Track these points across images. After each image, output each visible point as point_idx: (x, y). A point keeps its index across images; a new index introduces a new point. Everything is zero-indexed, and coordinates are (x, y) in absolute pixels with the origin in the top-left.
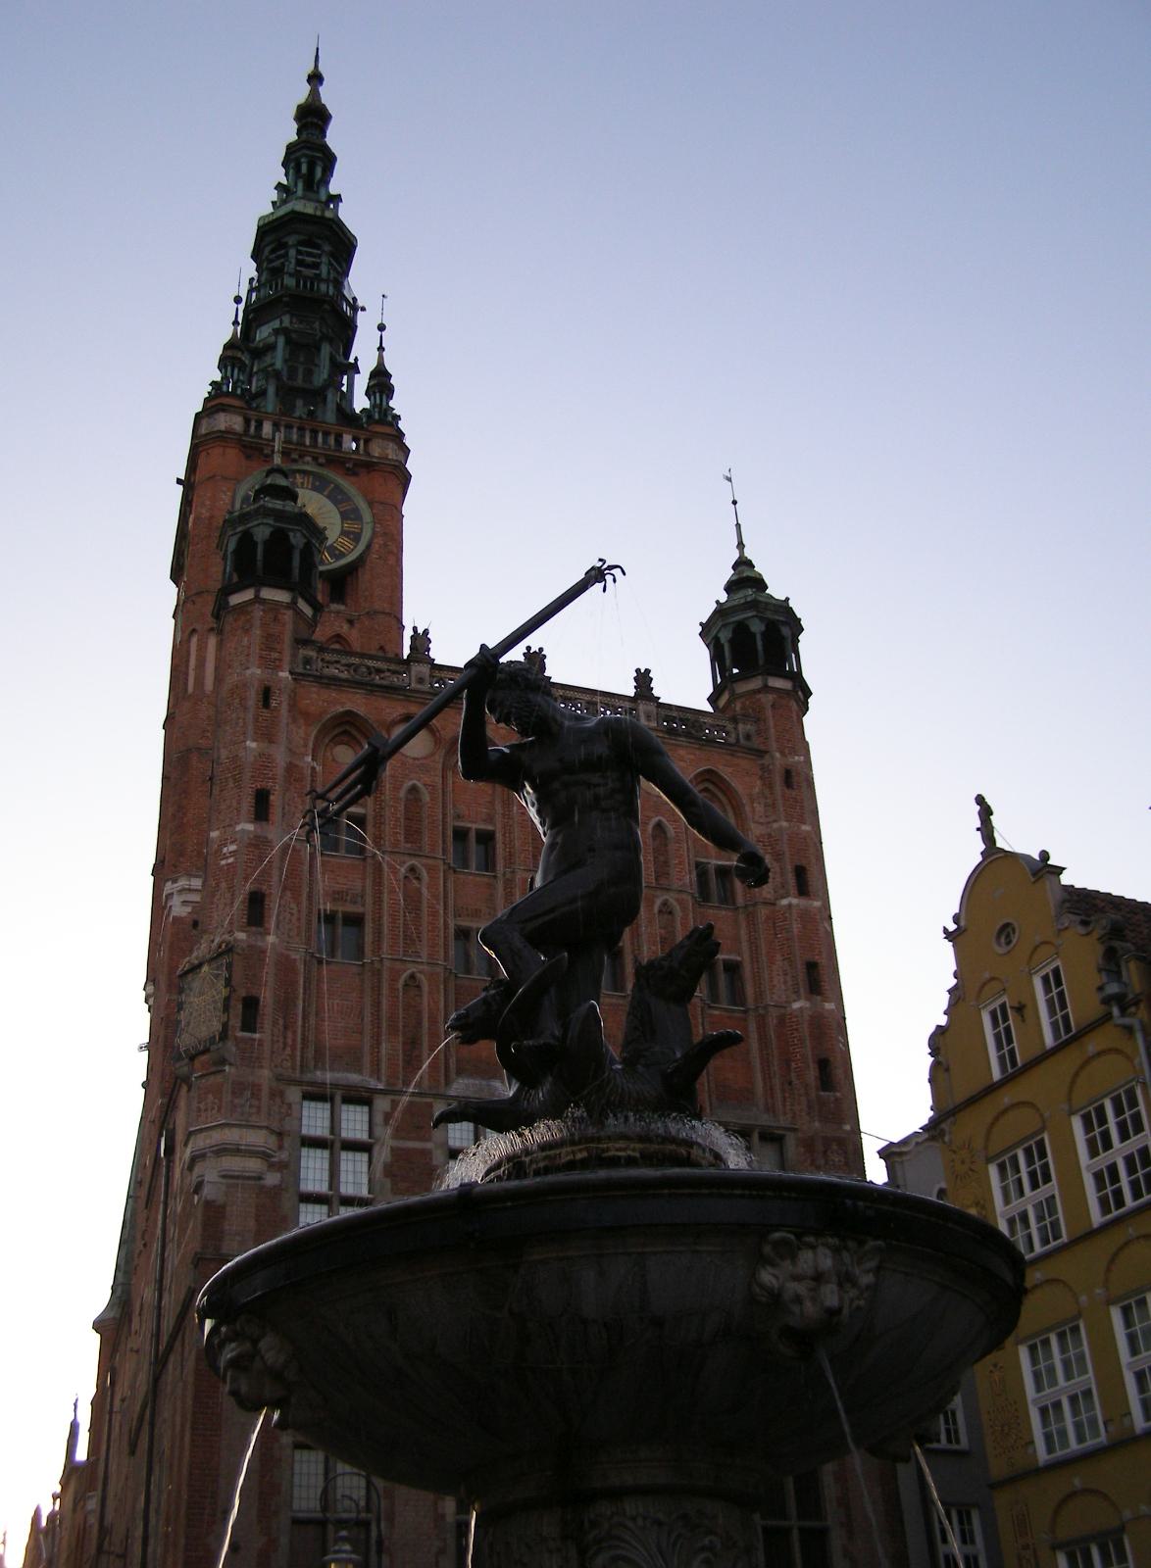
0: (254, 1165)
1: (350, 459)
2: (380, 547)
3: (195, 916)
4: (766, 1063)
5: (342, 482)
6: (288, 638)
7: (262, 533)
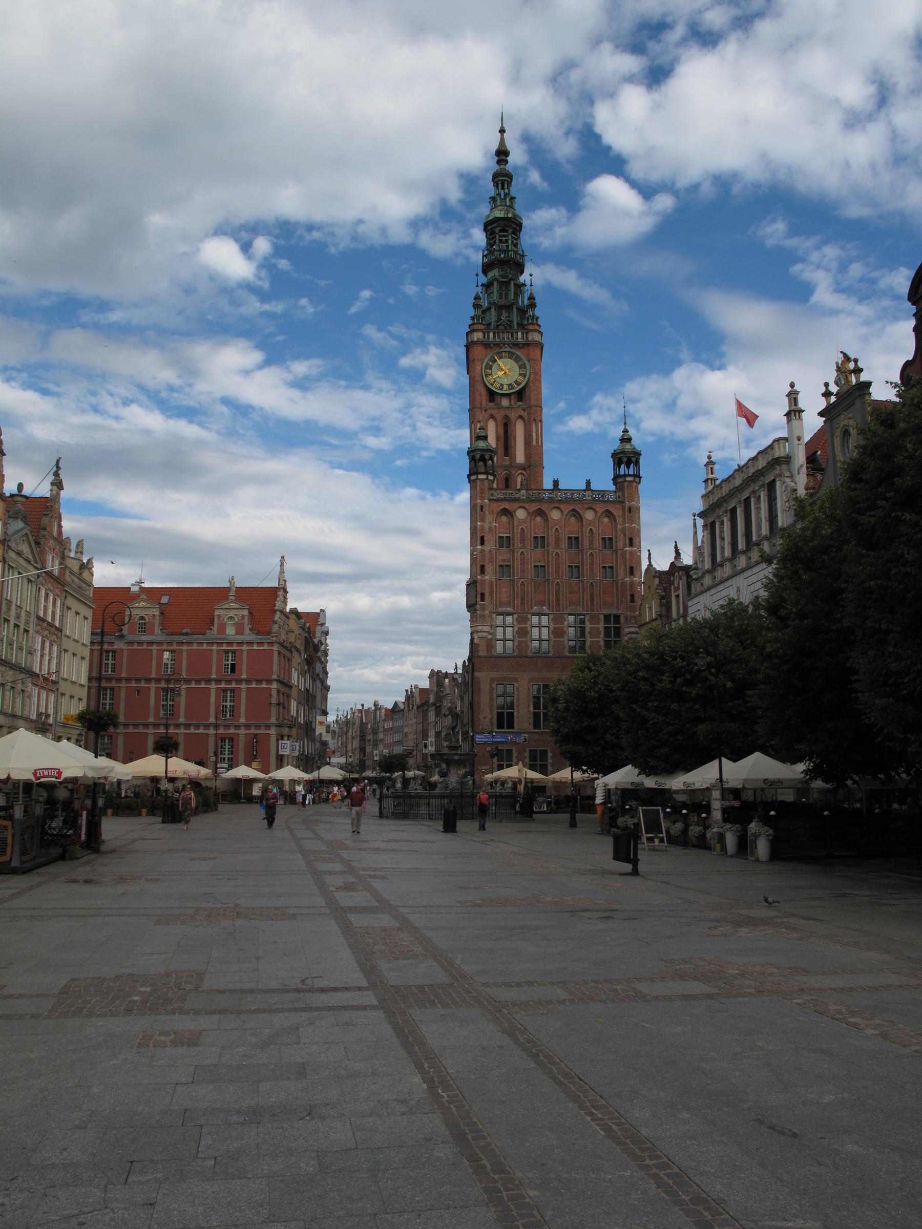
0: (485, 634)
4: (617, 595)
5: (518, 353)
6: (486, 489)
7: (478, 457)
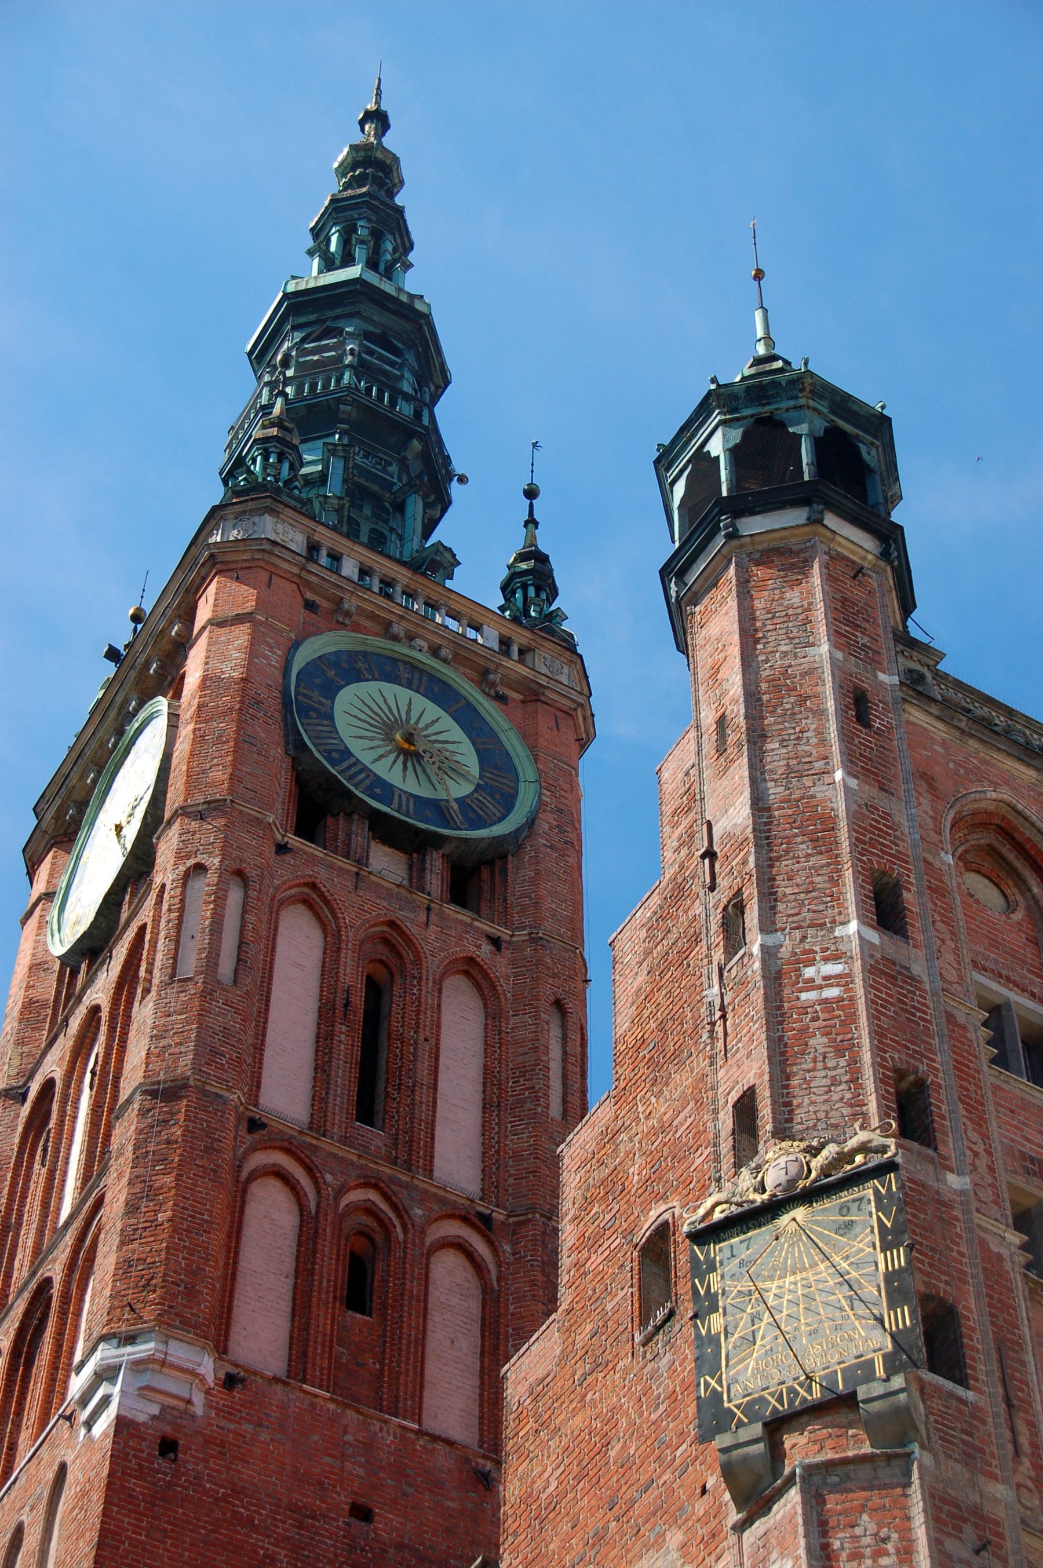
1: (499, 665)
2: (551, 828)
3: (167, 1429)
